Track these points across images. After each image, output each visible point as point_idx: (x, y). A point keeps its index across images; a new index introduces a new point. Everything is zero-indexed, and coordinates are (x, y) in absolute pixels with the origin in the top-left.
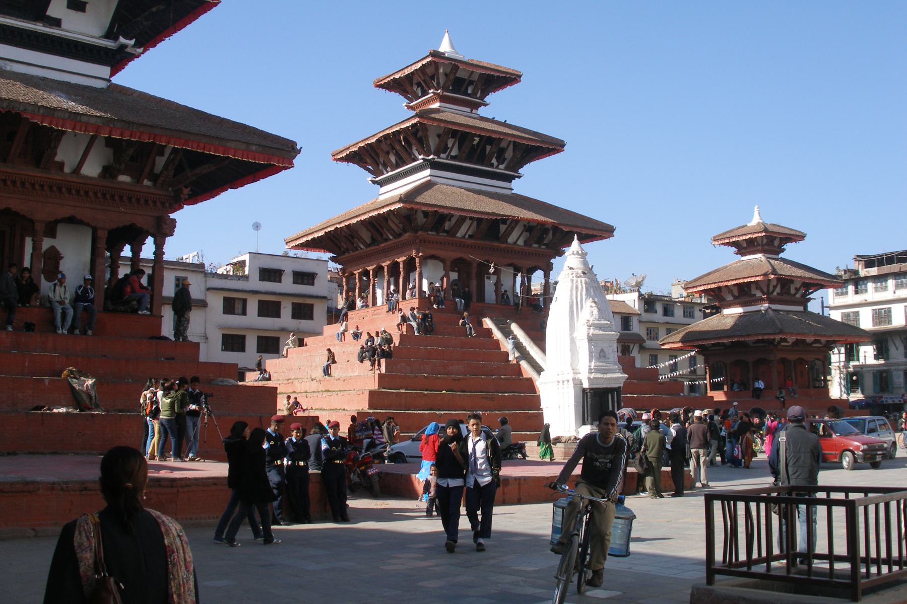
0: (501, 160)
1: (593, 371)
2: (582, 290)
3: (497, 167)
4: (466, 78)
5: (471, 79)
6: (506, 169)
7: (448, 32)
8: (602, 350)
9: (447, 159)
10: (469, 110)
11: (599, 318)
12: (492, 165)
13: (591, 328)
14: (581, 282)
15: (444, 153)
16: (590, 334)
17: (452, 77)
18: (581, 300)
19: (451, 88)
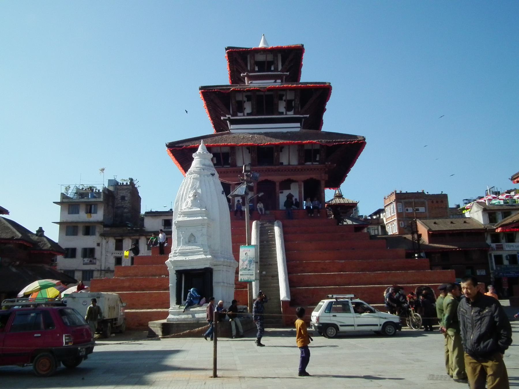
0: (289, 108)
1: (177, 255)
2: (189, 185)
3: (286, 114)
4: (265, 60)
5: (268, 60)
6: (295, 114)
7: (264, 35)
8: (192, 235)
9: (244, 116)
10: (273, 81)
11: (191, 207)
12: (282, 113)
13: (181, 216)
14: (190, 178)
15: (241, 112)
16: (176, 222)
17: (252, 62)
18: (186, 193)
19: (257, 69)
